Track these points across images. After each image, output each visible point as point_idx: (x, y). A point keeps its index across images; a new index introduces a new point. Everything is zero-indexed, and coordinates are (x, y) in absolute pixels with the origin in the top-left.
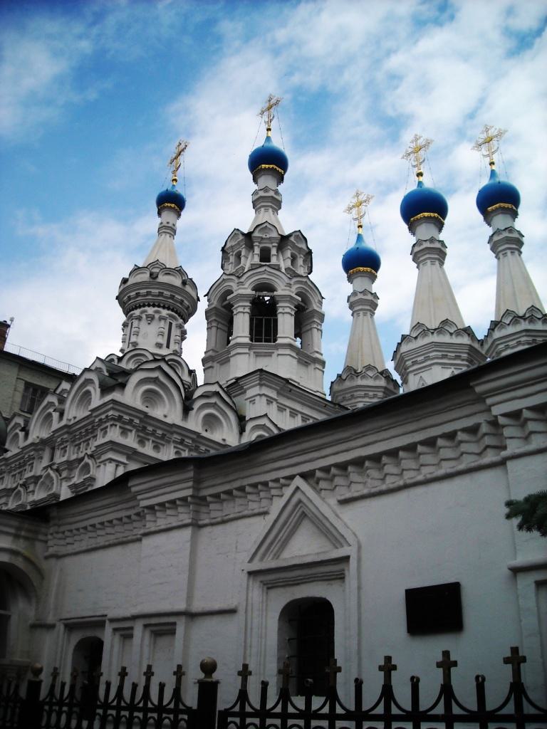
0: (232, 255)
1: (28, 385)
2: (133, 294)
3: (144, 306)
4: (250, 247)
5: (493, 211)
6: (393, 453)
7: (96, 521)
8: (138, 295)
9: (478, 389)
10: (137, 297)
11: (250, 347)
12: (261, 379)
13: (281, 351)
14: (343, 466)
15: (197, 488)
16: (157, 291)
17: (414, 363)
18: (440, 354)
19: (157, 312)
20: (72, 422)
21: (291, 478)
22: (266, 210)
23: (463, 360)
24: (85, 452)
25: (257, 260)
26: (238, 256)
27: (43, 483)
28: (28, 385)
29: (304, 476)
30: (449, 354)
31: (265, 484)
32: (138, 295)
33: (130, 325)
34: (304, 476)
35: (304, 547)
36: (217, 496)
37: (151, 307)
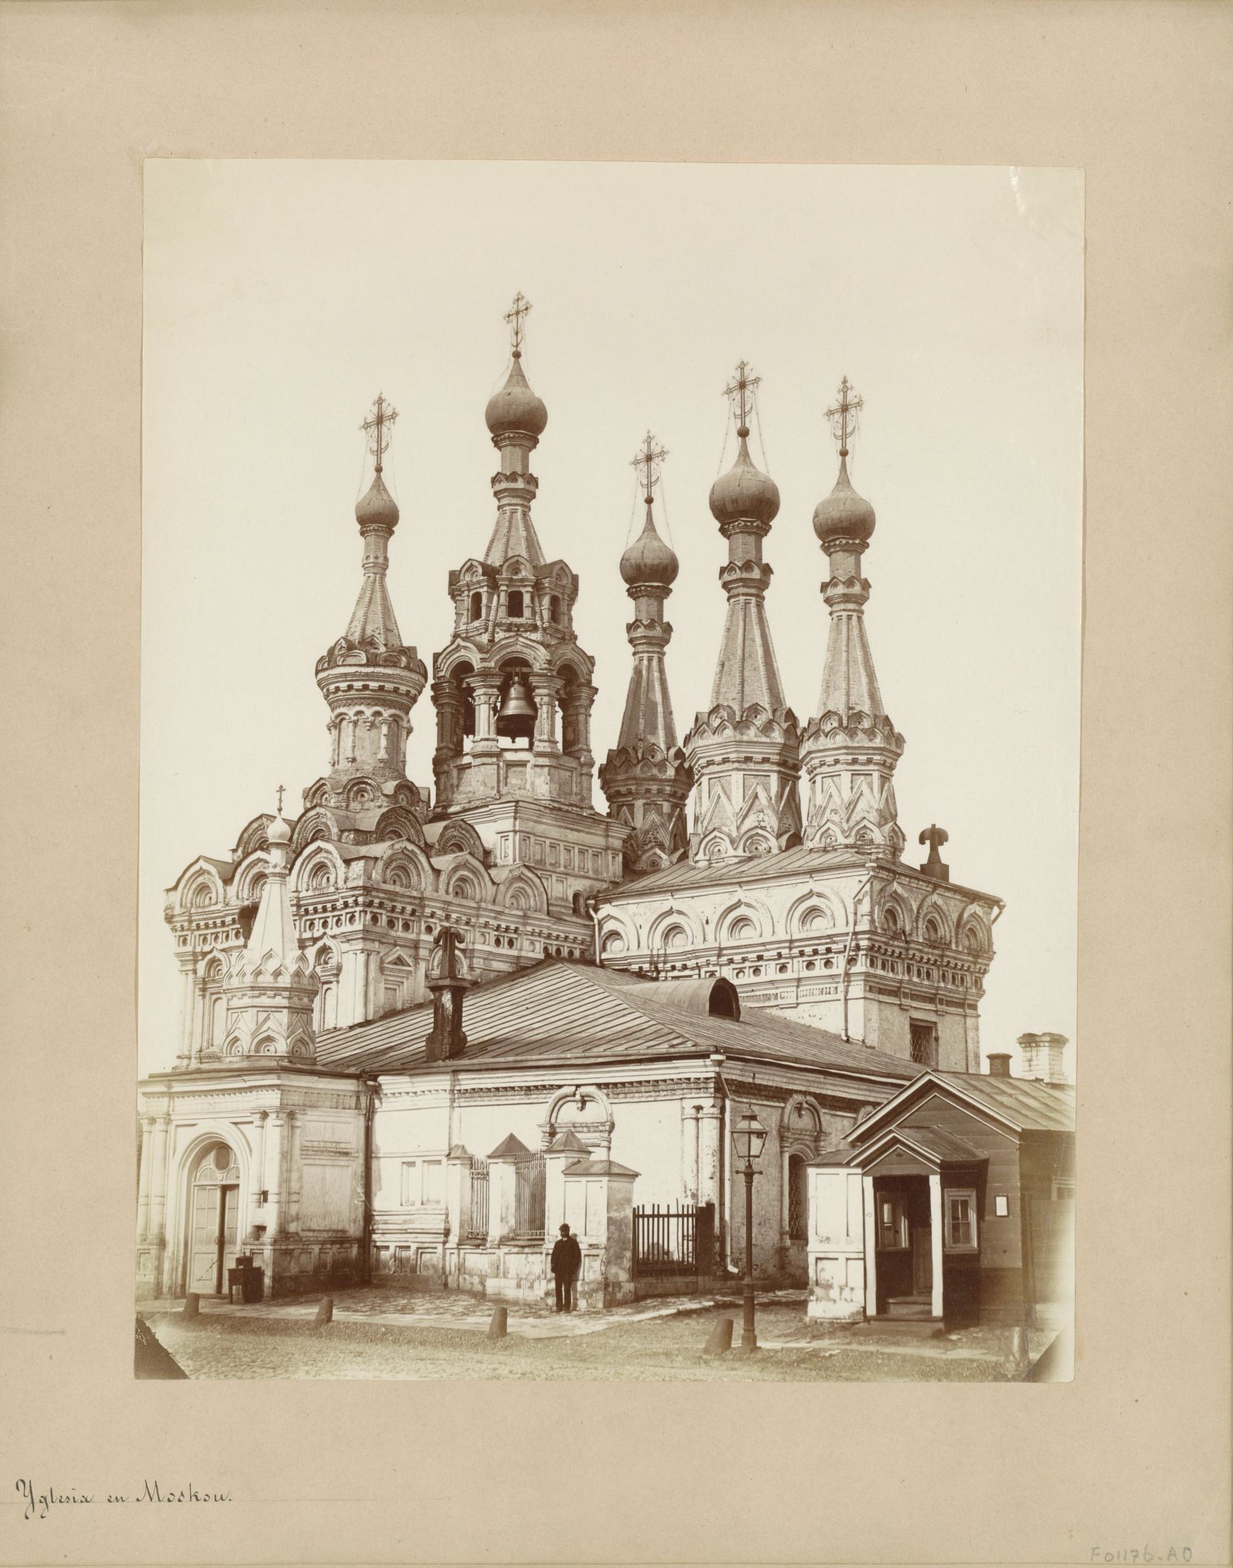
0: (468, 596)
2: (343, 686)
7: (418, 1090)
8: (350, 688)
17: (710, 763)
23: (773, 763)
24: (322, 931)
25: (503, 611)
26: (477, 598)
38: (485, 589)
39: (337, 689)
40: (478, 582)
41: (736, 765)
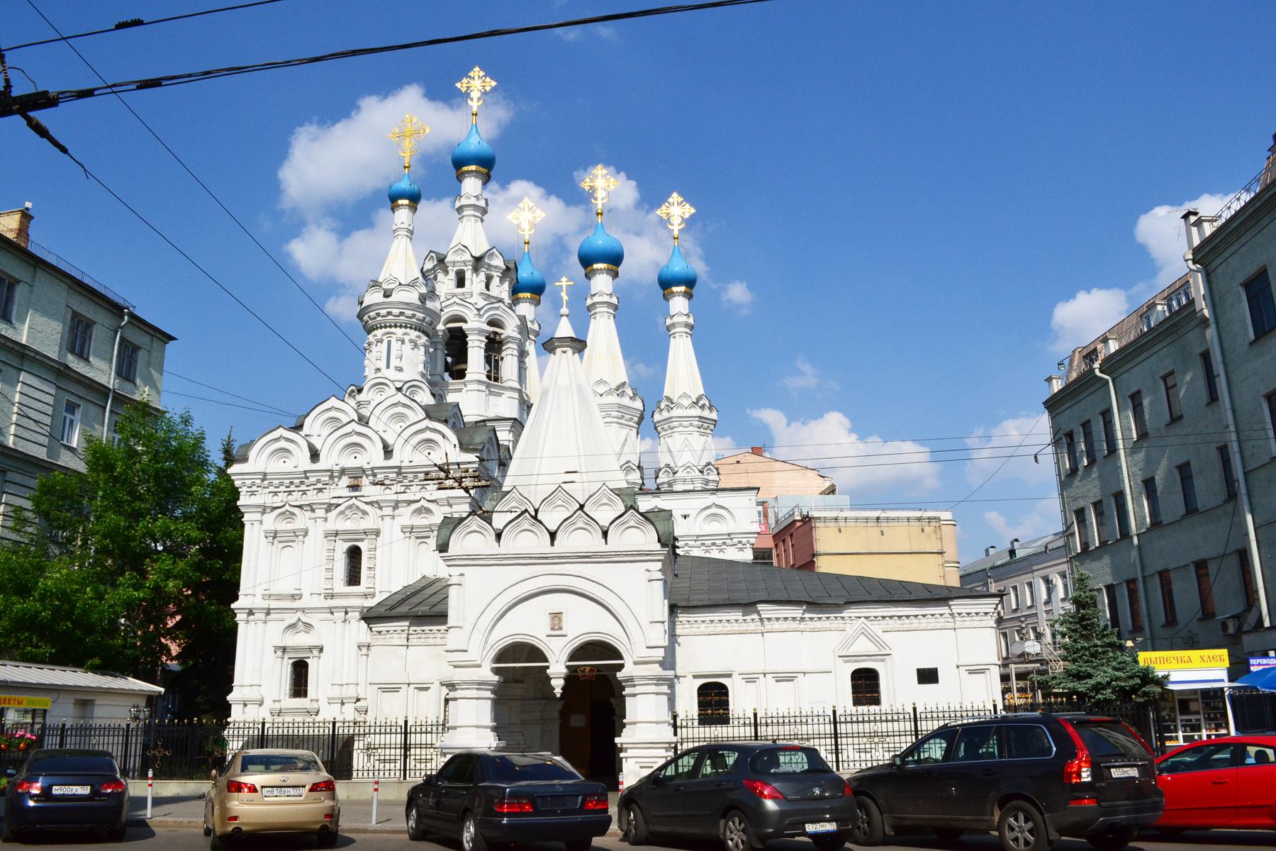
1: (75, 315)
2: (396, 311)
3: (406, 327)
4: (476, 270)
5: (677, 292)
6: (908, 617)
7: (716, 619)
8: (402, 314)
9: (950, 603)
10: (399, 316)
11: (488, 386)
12: (512, 427)
13: (508, 394)
14: (884, 617)
15: (803, 614)
16: (422, 315)
18: (620, 414)
19: (418, 337)
20: (406, 464)
21: (860, 618)
22: (470, 220)
27: (342, 513)
28: (75, 315)
29: (865, 617)
30: (626, 416)
31: (843, 618)
32: (402, 314)
33: (385, 343)
34: (865, 617)
35: (863, 646)
36: (812, 619)
37: (413, 331)
38: (470, 267)
39: (389, 313)
40: (464, 262)
41: (615, 420)
